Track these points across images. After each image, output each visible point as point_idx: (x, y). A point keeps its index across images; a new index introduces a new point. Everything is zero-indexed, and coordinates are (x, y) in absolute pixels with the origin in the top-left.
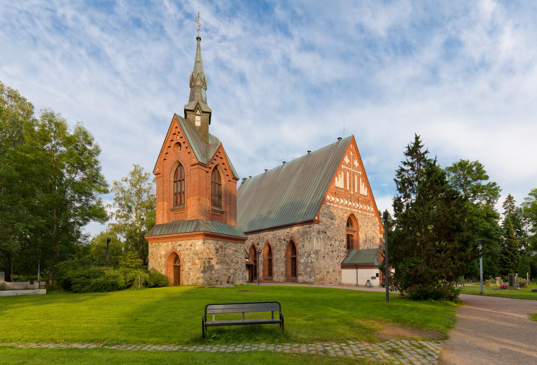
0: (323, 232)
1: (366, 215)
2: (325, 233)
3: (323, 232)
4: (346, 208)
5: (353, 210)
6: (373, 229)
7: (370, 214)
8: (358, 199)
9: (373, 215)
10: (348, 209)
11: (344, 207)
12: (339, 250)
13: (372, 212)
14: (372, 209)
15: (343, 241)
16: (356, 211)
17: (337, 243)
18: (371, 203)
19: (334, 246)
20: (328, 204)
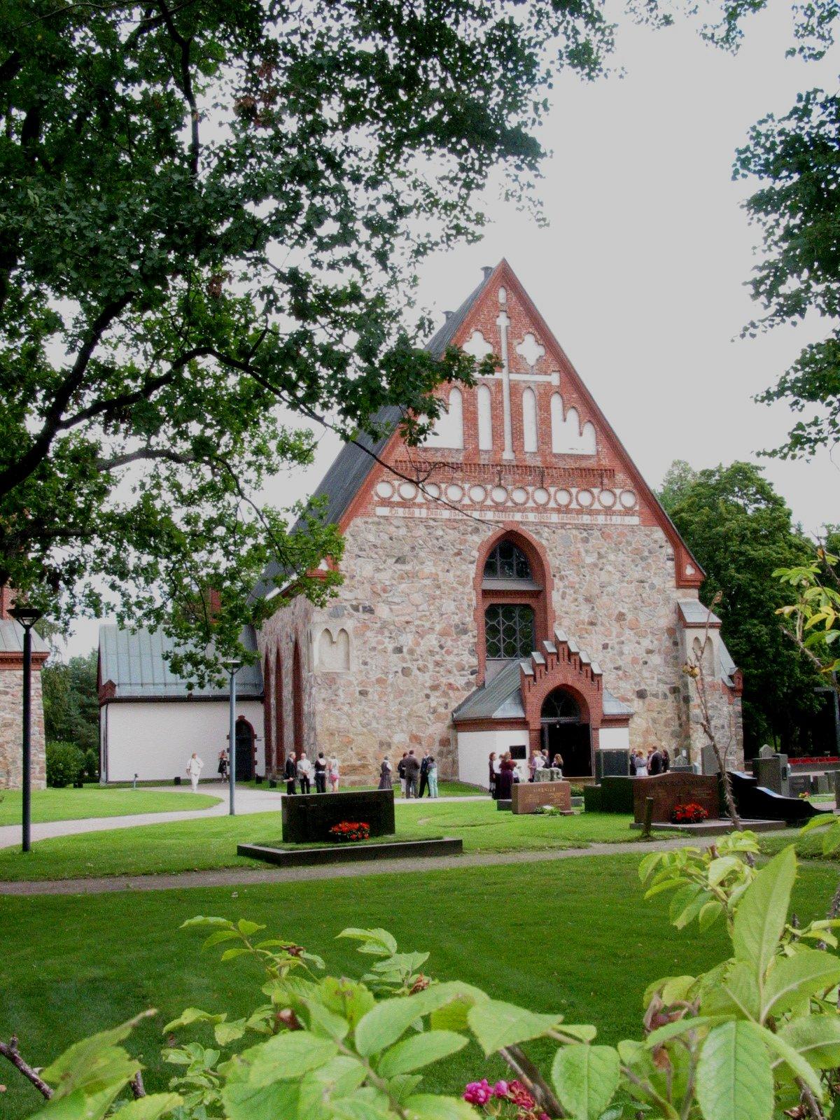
0: (356, 609)
1: (587, 528)
2: (370, 610)
3: (364, 608)
4: (476, 515)
5: (518, 517)
6: (637, 573)
7: (616, 520)
8: (544, 472)
9: (635, 520)
10: (489, 516)
12: (437, 664)
13: (628, 511)
14: (629, 500)
15: (465, 632)
16: (532, 517)
17: (432, 641)
18: (620, 476)
19: (411, 652)
20: (383, 511)
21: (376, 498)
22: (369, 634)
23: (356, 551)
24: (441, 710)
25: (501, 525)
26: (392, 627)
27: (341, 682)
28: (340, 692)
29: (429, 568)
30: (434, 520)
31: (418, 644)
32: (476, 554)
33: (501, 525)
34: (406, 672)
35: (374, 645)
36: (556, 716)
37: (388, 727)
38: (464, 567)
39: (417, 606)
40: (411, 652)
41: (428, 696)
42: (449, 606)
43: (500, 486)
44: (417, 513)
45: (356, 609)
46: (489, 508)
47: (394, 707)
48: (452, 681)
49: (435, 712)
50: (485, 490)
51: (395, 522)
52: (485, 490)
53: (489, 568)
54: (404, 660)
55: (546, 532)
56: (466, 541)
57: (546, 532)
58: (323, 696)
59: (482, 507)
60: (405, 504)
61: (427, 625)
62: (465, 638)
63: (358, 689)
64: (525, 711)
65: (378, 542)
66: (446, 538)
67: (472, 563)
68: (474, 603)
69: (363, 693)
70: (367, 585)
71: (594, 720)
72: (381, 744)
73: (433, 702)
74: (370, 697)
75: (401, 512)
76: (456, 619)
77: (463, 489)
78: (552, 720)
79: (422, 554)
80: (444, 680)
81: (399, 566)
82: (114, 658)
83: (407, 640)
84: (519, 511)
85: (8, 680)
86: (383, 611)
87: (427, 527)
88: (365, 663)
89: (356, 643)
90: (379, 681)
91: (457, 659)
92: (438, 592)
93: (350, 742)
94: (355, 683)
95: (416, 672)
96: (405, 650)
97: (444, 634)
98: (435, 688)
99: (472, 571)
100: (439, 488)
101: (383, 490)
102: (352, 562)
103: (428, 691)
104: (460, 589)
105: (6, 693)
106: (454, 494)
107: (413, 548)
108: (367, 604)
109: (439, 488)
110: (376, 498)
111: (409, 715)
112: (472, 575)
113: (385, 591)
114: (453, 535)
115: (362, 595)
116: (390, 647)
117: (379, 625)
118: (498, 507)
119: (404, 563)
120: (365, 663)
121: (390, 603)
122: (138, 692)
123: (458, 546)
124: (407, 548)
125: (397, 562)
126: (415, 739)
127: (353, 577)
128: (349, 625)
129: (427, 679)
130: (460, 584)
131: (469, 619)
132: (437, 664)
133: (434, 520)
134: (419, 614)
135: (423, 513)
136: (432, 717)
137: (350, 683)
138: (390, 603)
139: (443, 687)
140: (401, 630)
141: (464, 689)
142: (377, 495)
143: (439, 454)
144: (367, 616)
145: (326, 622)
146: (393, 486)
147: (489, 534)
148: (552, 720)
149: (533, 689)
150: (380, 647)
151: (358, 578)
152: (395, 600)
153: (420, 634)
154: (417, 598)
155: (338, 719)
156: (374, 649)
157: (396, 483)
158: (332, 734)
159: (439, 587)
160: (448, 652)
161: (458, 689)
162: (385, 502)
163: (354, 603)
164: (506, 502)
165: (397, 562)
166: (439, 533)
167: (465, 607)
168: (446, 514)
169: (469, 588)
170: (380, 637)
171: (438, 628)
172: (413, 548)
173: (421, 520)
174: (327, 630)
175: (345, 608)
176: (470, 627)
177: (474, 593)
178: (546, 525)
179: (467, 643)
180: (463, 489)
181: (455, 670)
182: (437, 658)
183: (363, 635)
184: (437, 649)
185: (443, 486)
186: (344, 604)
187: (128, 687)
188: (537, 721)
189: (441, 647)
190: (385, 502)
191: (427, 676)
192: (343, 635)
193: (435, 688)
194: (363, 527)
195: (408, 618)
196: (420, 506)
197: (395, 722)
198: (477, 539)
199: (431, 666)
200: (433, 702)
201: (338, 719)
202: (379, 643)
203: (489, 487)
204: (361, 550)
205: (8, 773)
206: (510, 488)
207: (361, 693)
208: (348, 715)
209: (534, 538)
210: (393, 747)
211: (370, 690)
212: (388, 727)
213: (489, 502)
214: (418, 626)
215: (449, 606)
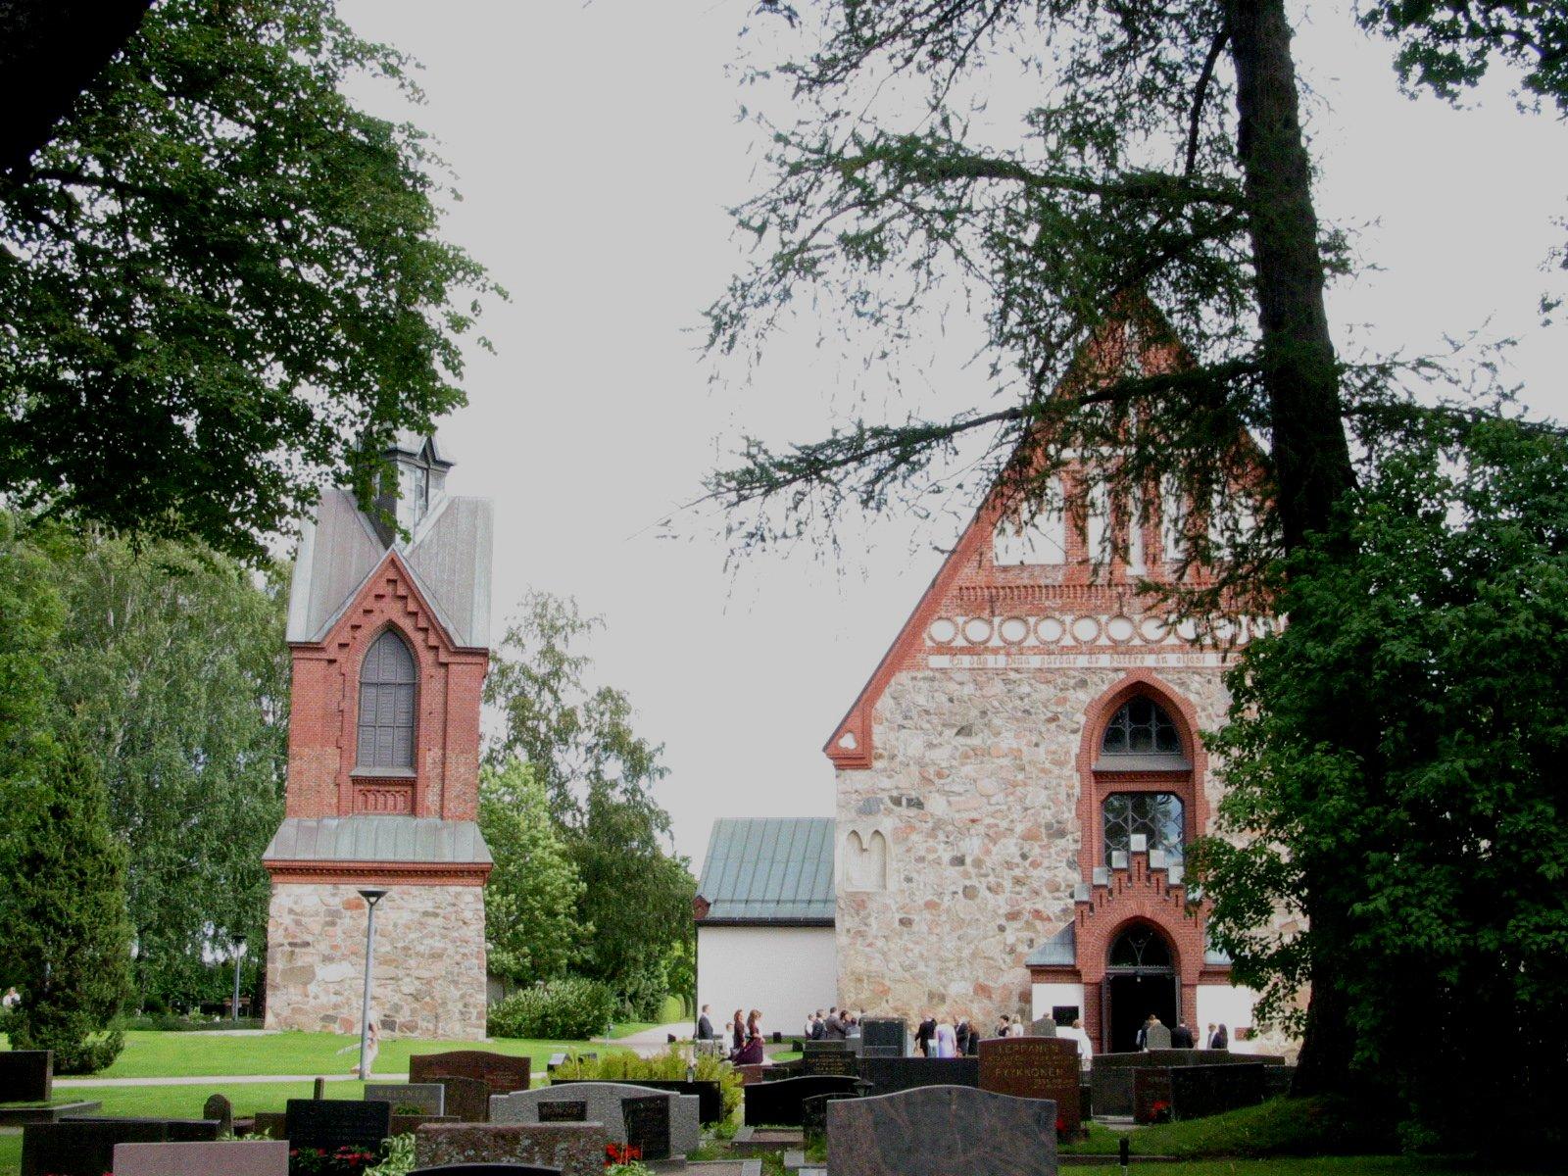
0: (897, 802)
2: (920, 805)
4: (1082, 661)
5: (1150, 661)
10: (1104, 660)
11: (1055, 662)
12: (1018, 881)
15: (1062, 834)
16: (1173, 660)
17: (1010, 847)
19: (978, 863)
21: (929, 643)
22: (915, 837)
23: (900, 720)
24: (1023, 948)
25: (1122, 675)
26: (950, 828)
27: (872, 906)
28: (872, 921)
29: (1008, 741)
30: (1017, 671)
31: (988, 852)
32: (1082, 719)
33: (1122, 675)
34: (969, 892)
35: (922, 853)
36: (1135, 964)
37: (941, 972)
38: (1062, 739)
39: (988, 796)
40: (978, 863)
41: (1002, 929)
42: (1037, 796)
43: (1120, 615)
44: (991, 661)
45: (897, 802)
46: (1103, 650)
47: (950, 943)
48: (1039, 906)
49: (1012, 951)
50: (1098, 622)
51: (958, 677)
52: (1098, 622)
53: (1112, 739)
54: (966, 875)
55: (1196, 682)
56: (1065, 700)
57: (1196, 682)
58: (847, 925)
59: (1092, 648)
60: (973, 649)
61: (1004, 824)
62: (1061, 843)
63: (898, 916)
64: (1075, 955)
65: (931, 706)
66: (1035, 696)
67: (1074, 732)
68: (1077, 791)
69: (905, 922)
70: (914, 769)
71: (1188, 968)
72: (931, 996)
73: (1010, 937)
74: (915, 928)
75: (966, 661)
76: (1047, 816)
77: (1062, 623)
78: (1126, 969)
79: (997, 721)
80: (1028, 906)
81: (961, 739)
82: (778, 858)
83: (972, 846)
84: (1152, 651)
85: (439, 898)
86: (936, 805)
87: (1006, 682)
88: (909, 880)
89: (895, 850)
90: (930, 905)
91: (1047, 875)
92: (1020, 776)
93: (886, 992)
94: (894, 908)
95: (984, 892)
96: (968, 860)
97: (1029, 836)
98: (1013, 916)
99: (1075, 743)
100: (1026, 622)
101: (940, 630)
102: (892, 735)
103: (1003, 921)
104: (1056, 771)
105: (436, 915)
106: (1049, 630)
107: (984, 713)
108: (914, 794)
109: (1026, 622)
110: (929, 643)
111: (974, 955)
112: (1075, 749)
113: (940, 775)
114: (1046, 692)
115: (906, 782)
116: (946, 857)
117: (930, 825)
118: (1117, 647)
119: (969, 734)
120: (909, 880)
121: (948, 793)
122: (738, 912)
123: (1054, 708)
124: (975, 713)
125: (958, 733)
126: (982, 990)
127: (893, 757)
128: (887, 824)
129: (1002, 903)
130: (1055, 763)
131: (1069, 815)
132: (1018, 881)
133: (1017, 671)
134: (991, 809)
135: (1001, 661)
136: (1008, 959)
137: (887, 907)
138: (948, 793)
139: (1026, 916)
140: (963, 832)
141: (1059, 919)
142: (932, 638)
143: (1025, 575)
144: (913, 812)
145: (853, 821)
146: (956, 625)
147: (1103, 687)
148: (1126, 969)
149: (1088, 923)
150: (931, 857)
151: (900, 758)
152: (956, 788)
153: (993, 837)
154: (988, 785)
155: (869, 958)
156: (921, 859)
157: (960, 620)
158: (860, 980)
159: (1022, 769)
160: (1035, 865)
161: (1049, 919)
162: (943, 648)
163: (895, 794)
164: (1131, 639)
165: (958, 733)
166: (1025, 689)
167: (1063, 797)
168: (1035, 662)
169: (1070, 770)
170: (931, 842)
171: (1019, 828)
172: (984, 713)
173: (997, 672)
174: (854, 832)
175: (881, 800)
176: (1069, 827)
177: (1077, 777)
178: (1197, 671)
179: (1065, 851)
180: (1062, 623)
181: (1045, 892)
182: (1018, 872)
183: (906, 839)
184: (1018, 860)
185: (1032, 620)
186: (880, 795)
187: (758, 906)
188: (1098, 968)
189: (1024, 857)
190: (943, 648)
191: (1001, 899)
192: (878, 839)
193: (1013, 916)
194: (909, 684)
195: (974, 815)
196: (995, 651)
197: (952, 965)
198: (1083, 697)
199: (1008, 884)
200: (1010, 937)
201: (869, 958)
202: (929, 850)
203: (1104, 618)
204: (906, 718)
205: (437, 1017)
206: (1137, 618)
207: (902, 922)
208: (884, 954)
209: (1175, 691)
210: (949, 1001)
211: (916, 918)
212: (941, 972)
213: (1103, 641)
214: (989, 826)
215: (1037, 796)
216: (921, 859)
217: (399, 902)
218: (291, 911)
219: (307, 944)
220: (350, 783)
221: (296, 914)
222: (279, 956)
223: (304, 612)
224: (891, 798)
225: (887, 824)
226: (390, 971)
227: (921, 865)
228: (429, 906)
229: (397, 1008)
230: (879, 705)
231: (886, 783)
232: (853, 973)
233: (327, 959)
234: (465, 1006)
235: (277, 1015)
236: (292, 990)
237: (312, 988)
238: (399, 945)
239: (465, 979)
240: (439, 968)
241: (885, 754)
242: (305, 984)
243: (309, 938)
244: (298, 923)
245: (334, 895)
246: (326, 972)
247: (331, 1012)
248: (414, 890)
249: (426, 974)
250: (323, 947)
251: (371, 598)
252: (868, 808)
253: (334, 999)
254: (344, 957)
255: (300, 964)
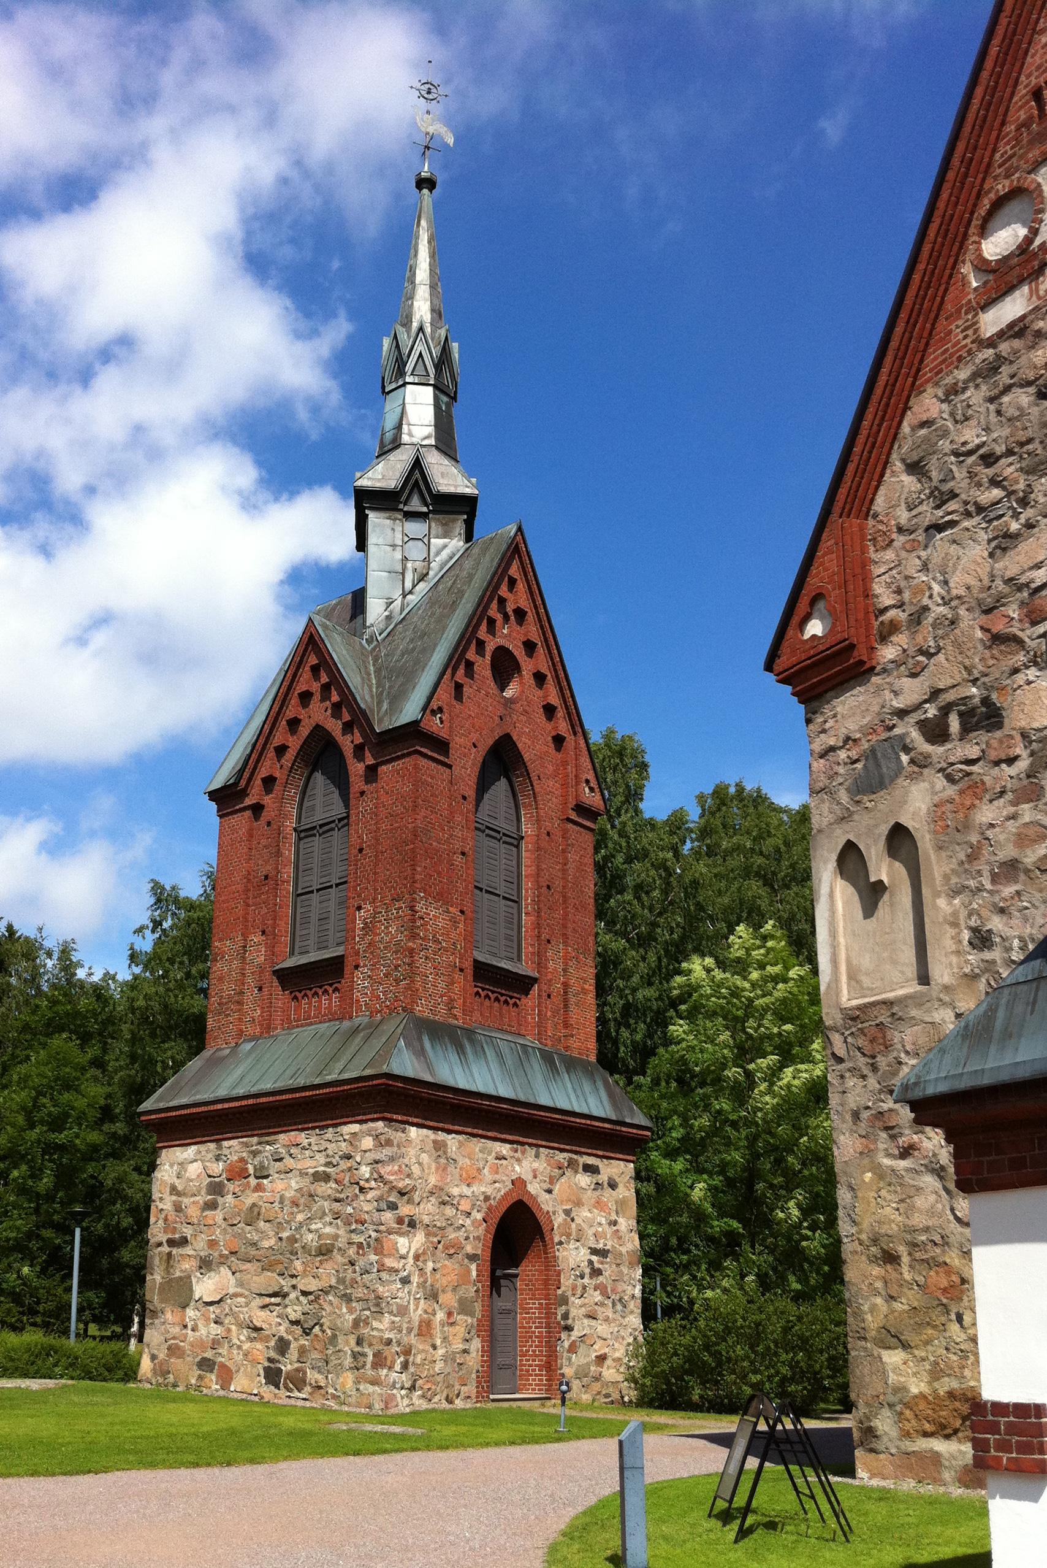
22: (986, 813)
35: (1008, 852)
58: (853, 1100)
89: (938, 866)
102: (913, 564)
156: (1010, 869)
183: (965, 826)
216: (1010, 869)
217: (289, 1162)
218: (174, 1190)
219: (184, 1242)
220: (276, 983)
221: (179, 1194)
222: (157, 1261)
223: (242, 749)
224: (922, 725)
225: (917, 801)
226: (272, 1280)
227: (1008, 890)
228: (318, 1164)
229: (283, 1346)
230: (880, 503)
231: (911, 691)
232: (875, 1241)
233: (206, 1265)
234: (359, 1342)
235: (153, 1357)
236: (169, 1315)
237: (190, 1313)
238: (285, 1235)
239: (360, 1292)
240: (328, 1273)
241: (902, 616)
242: (184, 1307)
243: (188, 1231)
244: (178, 1208)
245: (218, 1158)
246: (205, 1287)
247: (209, 1354)
248: (302, 1138)
249: (312, 1285)
250: (199, 1245)
251: (294, 700)
252: (874, 774)
253: (216, 1330)
254: (223, 1261)
255: (178, 1274)
